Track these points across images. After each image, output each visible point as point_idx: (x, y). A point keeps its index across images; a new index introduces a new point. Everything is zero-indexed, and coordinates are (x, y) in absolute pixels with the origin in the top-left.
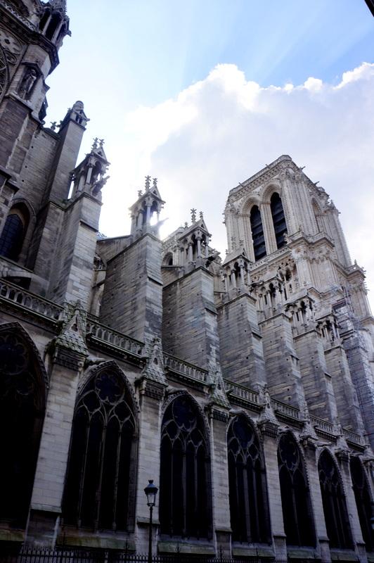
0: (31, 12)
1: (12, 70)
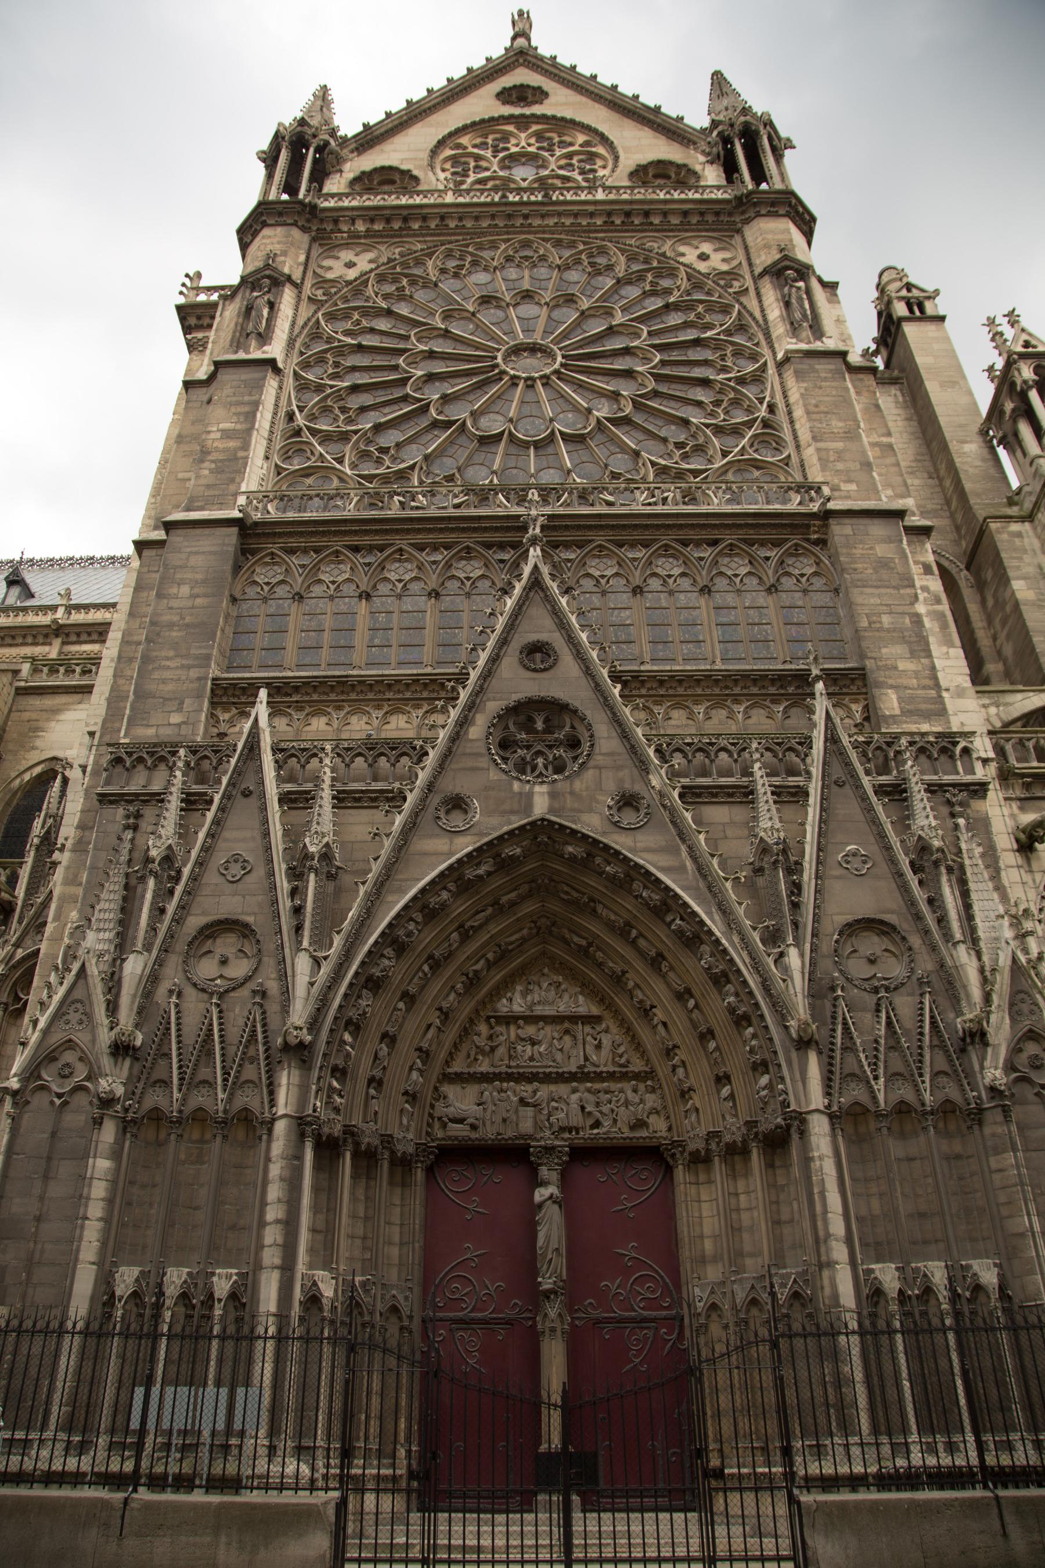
0: (698, 168)
1: (752, 304)
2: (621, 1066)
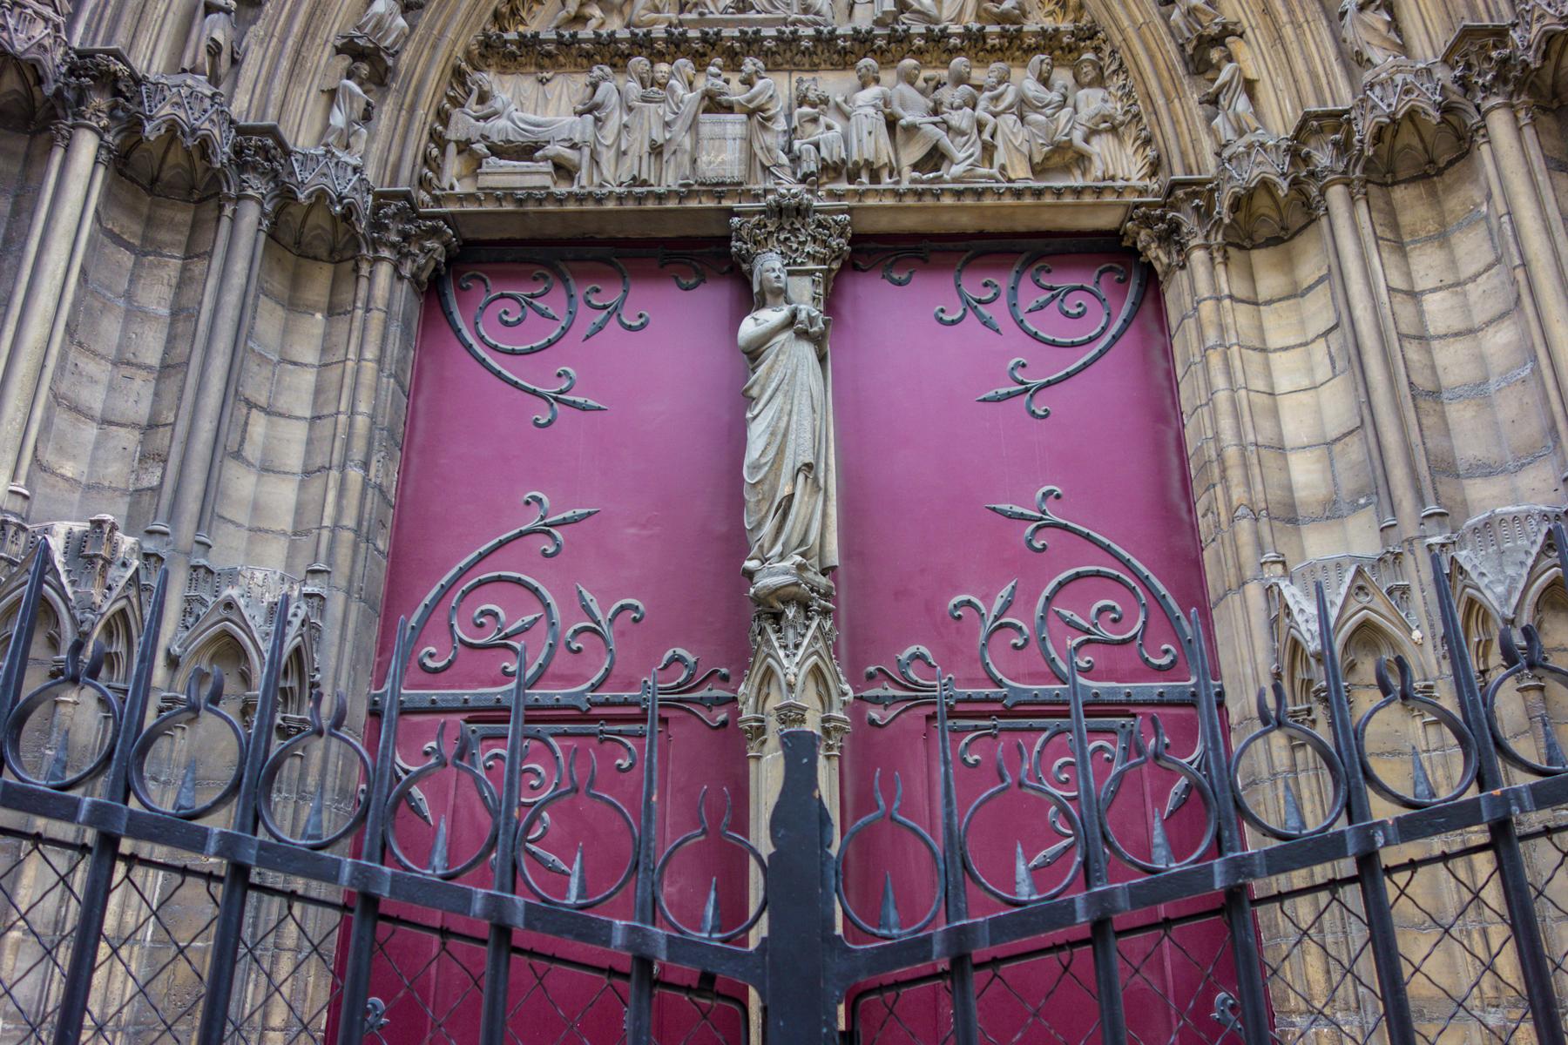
2: (1002, 18)
